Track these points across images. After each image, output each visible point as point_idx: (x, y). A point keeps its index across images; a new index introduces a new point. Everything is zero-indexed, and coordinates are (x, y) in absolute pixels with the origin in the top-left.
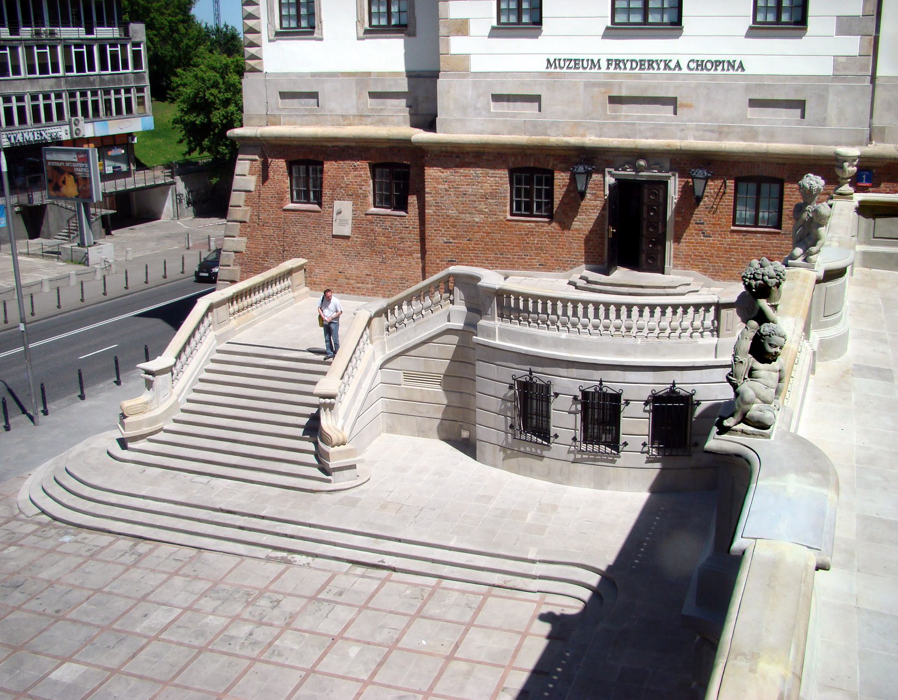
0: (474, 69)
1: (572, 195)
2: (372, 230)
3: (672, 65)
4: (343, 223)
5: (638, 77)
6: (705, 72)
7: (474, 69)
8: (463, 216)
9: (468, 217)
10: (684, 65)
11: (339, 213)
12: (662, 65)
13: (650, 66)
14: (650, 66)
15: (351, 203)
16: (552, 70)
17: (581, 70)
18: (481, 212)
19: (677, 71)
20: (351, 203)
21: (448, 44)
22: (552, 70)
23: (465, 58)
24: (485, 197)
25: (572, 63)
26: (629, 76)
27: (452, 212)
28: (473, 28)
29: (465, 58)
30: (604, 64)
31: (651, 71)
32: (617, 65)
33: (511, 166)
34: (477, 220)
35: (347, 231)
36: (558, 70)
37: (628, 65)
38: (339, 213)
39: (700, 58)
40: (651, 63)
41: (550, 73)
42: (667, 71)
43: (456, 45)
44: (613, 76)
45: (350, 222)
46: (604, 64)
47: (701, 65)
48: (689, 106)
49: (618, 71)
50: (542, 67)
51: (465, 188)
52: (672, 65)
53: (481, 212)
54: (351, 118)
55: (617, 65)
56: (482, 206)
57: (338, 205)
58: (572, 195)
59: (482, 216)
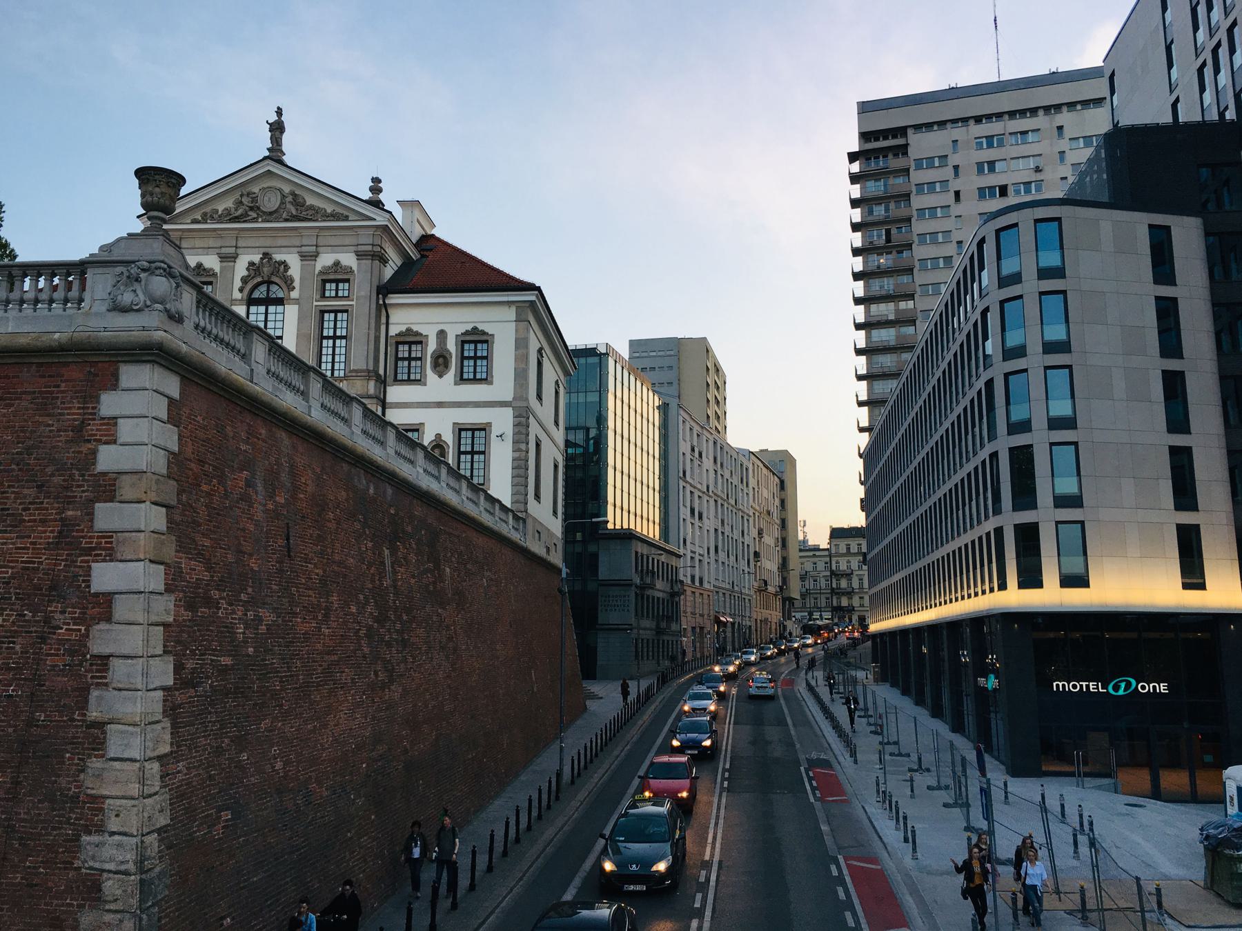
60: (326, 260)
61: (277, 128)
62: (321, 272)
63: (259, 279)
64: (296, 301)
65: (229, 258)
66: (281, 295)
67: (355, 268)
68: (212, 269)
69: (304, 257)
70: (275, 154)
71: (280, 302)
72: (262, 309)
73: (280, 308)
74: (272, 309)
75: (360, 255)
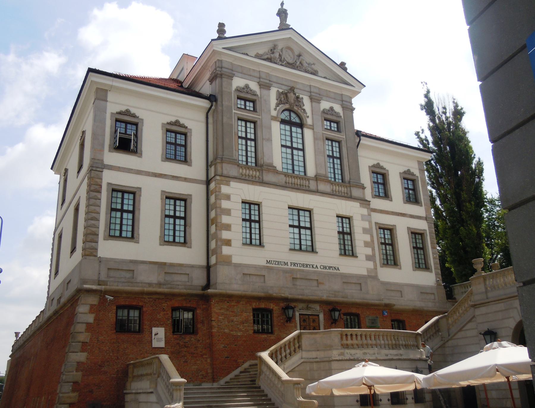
0: (235, 260)
1: (282, 321)
2: (178, 343)
3: (315, 266)
4: (159, 340)
5: (303, 271)
6: (326, 270)
7: (235, 260)
8: (232, 333)
9: (234, 333)
10: (319, 267)
11: (156, 335)
12: (311, 266)
13: (307, 266)
14: (307, 266)
15: (164, 329)
16: (268, 265)
17: (280, 266)
18: (240, 330)
19: (316, 269)
20: (164, 329)
21: (221, 249)
22: (268, 265)
23: (230, 257)
24: (242, 323)
25: (277, 263)
26: (300, 270)
27: (227, 331)
28: (233, 243)
29: (230, 257)
30: (289, 264)
31: (307, 269)
32: (294, 265)
33: (254, 307)
34: (239, 334)
35: (162, 344)
36: (271, 265)
37: (299, 265)
38: (156, 335)
39: (324, 265)
40: (307, 266)
41: (267, 266)
42: (313, 269)
43: (226, 250)
44: (293, 270)
45: (164, 339)
46: (289, 264)
47: (325, 267)
48: (323, 284)
49: (295, 267)
50: (263, 263)
51: (232, 318)
52: (315, 266)
53: (240, 330)
54: (154, 285)
55: (294, 265)
56: (241, 327)
57: (155, 330)
58: (282, 321)
59: (241, 333)
60: (325, 105)
61: (282, 14)
62: (324, 112)
63: (287, 106)
64: (312, 127)
65: (265, 86)
66: (297, 120)
67: (342, 114)
68: (255, 91)
69: (312, 99)
70: (284, 27)
71: (301, 125)
72: (288, 128)
73: (299, 130)
74: (294, 129)
75: (344, 108)
